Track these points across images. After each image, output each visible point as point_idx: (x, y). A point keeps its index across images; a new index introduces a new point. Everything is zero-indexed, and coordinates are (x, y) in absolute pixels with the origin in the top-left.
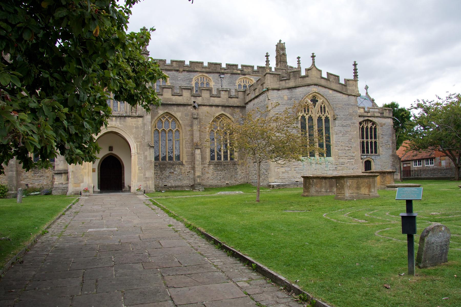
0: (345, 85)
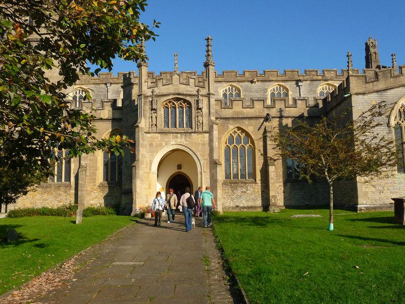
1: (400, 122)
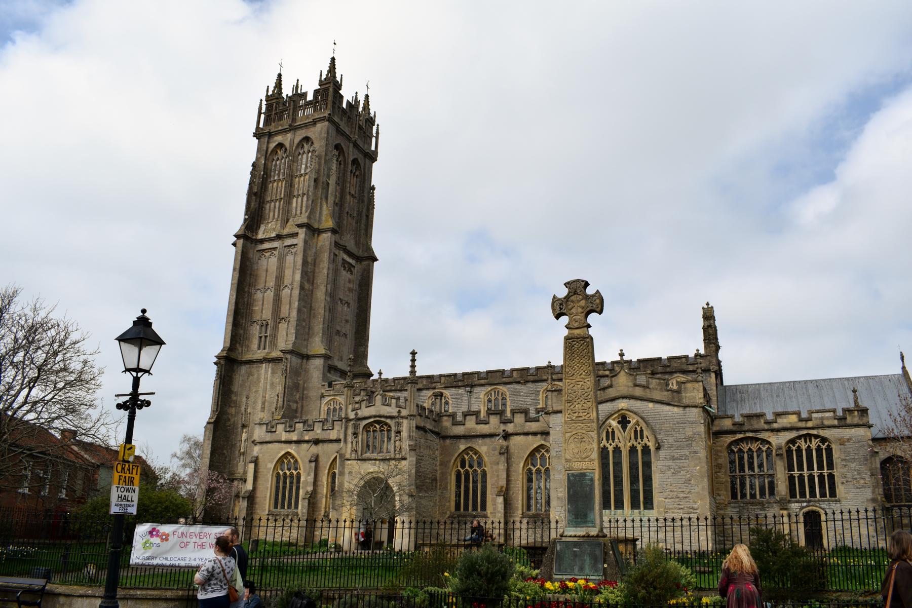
0: (678, 392)
1: (607, 445)
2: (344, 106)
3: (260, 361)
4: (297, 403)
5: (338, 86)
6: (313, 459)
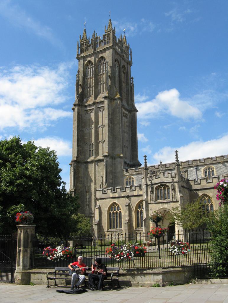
2: (117, 41)
3: (91, 162)
4: (112, 179)
5: (114, 32)
6: (127, 205)
